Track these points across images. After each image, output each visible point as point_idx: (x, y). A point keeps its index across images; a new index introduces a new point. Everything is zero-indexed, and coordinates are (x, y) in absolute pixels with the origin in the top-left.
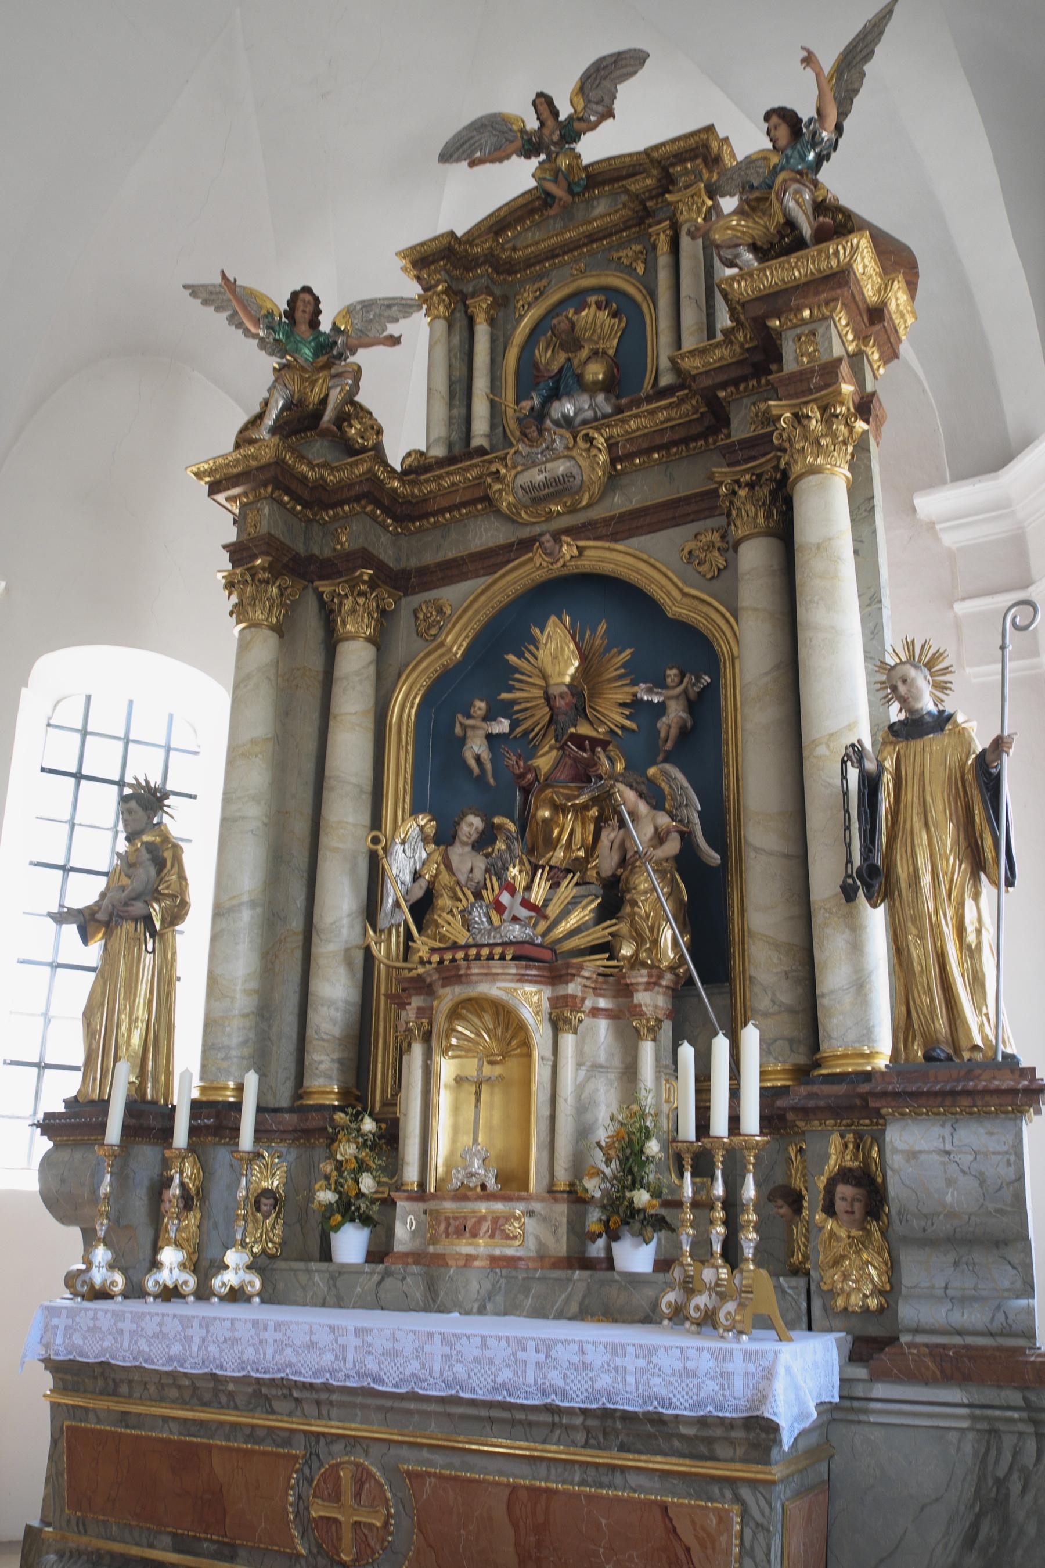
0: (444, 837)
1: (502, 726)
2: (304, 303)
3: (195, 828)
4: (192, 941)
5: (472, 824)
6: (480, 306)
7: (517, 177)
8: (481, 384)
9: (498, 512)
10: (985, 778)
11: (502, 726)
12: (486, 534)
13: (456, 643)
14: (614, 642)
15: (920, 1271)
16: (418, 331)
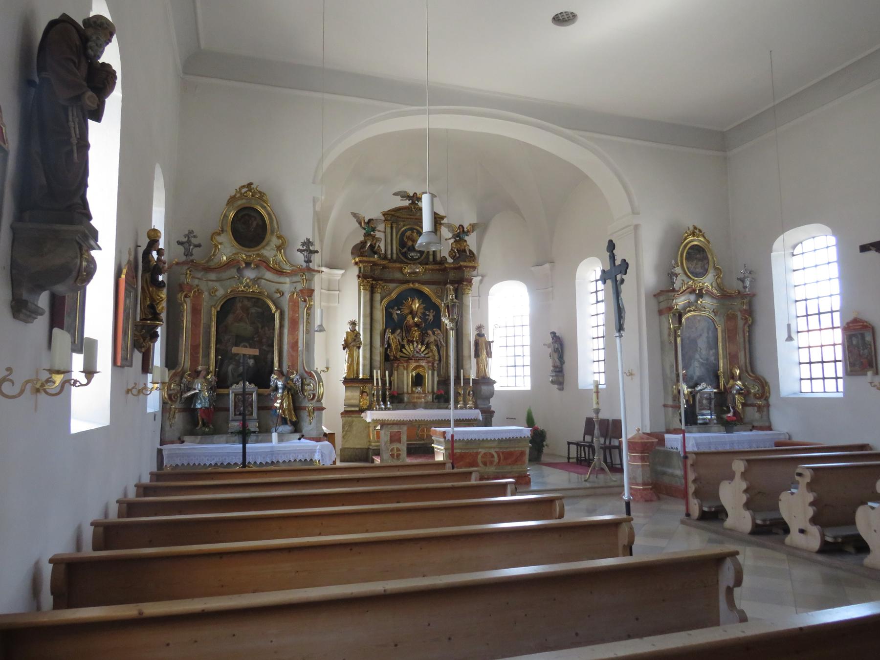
0: (393, 333)
1: (399, 312)
2: (370, 220)
3: (360, 329)
4: (361, 350)
5: (399, 331)
6: (394, 225)
7: (407, 203)
8: (394, 242)
9: (402, 272)
10: (489, 344)
11: (399, 312)
12: (398, 275)
13: (394, 295)
14: (423, 303)
15: (479, 402)
16: (381, 227)
